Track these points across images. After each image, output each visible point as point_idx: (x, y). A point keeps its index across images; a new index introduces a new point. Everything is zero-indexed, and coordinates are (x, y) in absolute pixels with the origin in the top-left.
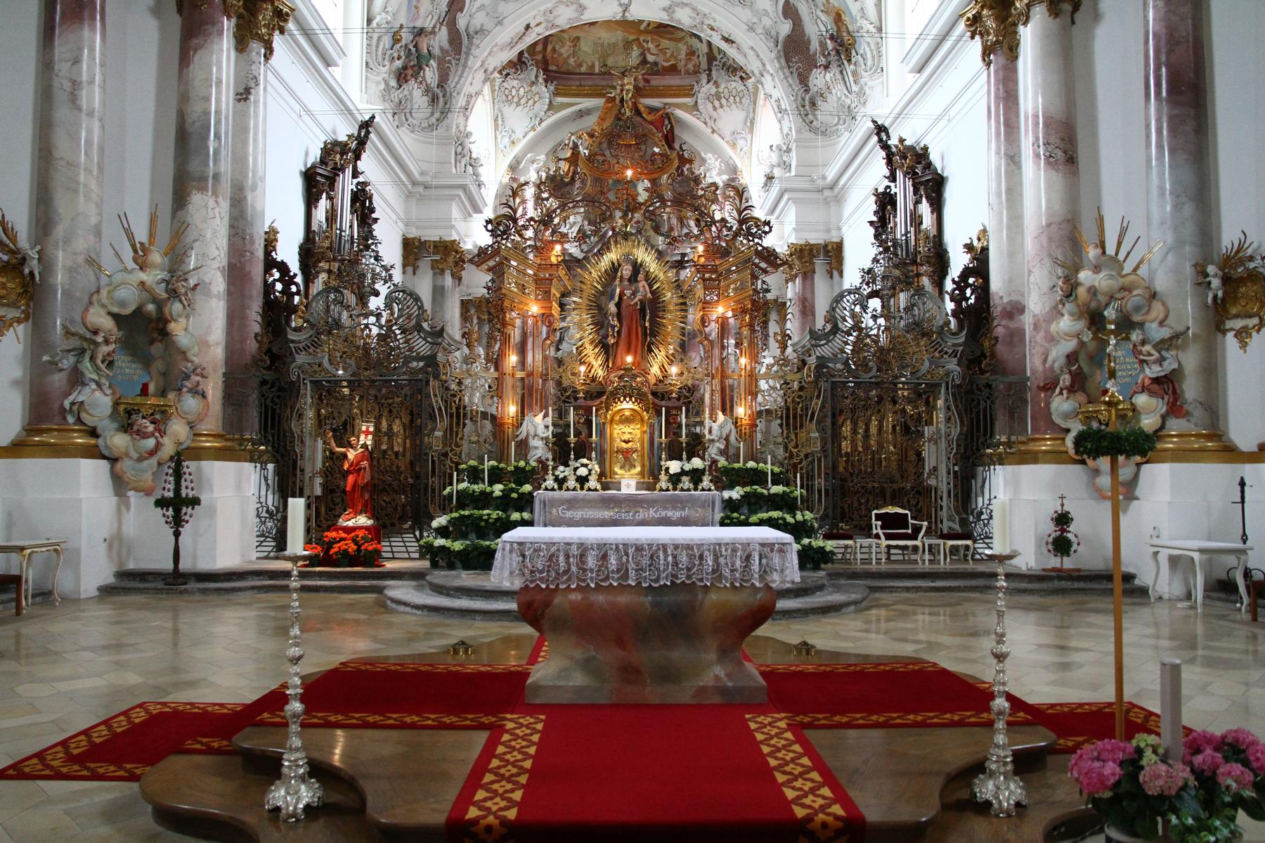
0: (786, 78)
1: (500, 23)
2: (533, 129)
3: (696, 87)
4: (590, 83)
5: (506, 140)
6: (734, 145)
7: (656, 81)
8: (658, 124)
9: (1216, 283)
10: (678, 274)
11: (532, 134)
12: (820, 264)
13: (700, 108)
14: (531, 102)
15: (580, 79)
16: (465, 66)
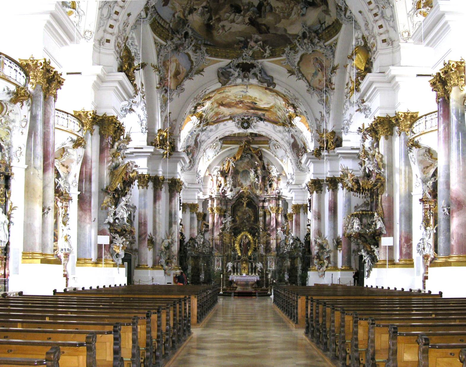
0: (292, 154)
1: (209, 138)
2: (215, 155)
3: (269, 141)
4: (233, 140)
5: (207, 160)
6: (282, 161)
7: (256, 139)
8: (257, 154)
9: (335, 242)
10: (263, 204)
11: (215, 157)
12: (302, 211)
13: (271, 148)
14: (215, 147)
15: (231, 139)
16: (199, 151)
